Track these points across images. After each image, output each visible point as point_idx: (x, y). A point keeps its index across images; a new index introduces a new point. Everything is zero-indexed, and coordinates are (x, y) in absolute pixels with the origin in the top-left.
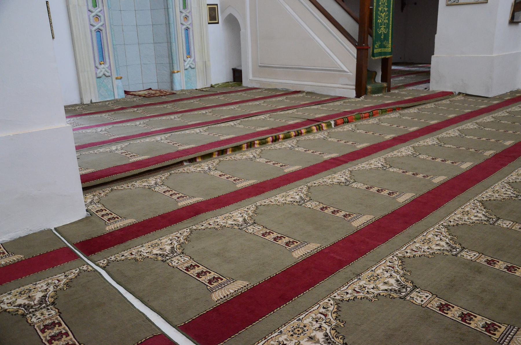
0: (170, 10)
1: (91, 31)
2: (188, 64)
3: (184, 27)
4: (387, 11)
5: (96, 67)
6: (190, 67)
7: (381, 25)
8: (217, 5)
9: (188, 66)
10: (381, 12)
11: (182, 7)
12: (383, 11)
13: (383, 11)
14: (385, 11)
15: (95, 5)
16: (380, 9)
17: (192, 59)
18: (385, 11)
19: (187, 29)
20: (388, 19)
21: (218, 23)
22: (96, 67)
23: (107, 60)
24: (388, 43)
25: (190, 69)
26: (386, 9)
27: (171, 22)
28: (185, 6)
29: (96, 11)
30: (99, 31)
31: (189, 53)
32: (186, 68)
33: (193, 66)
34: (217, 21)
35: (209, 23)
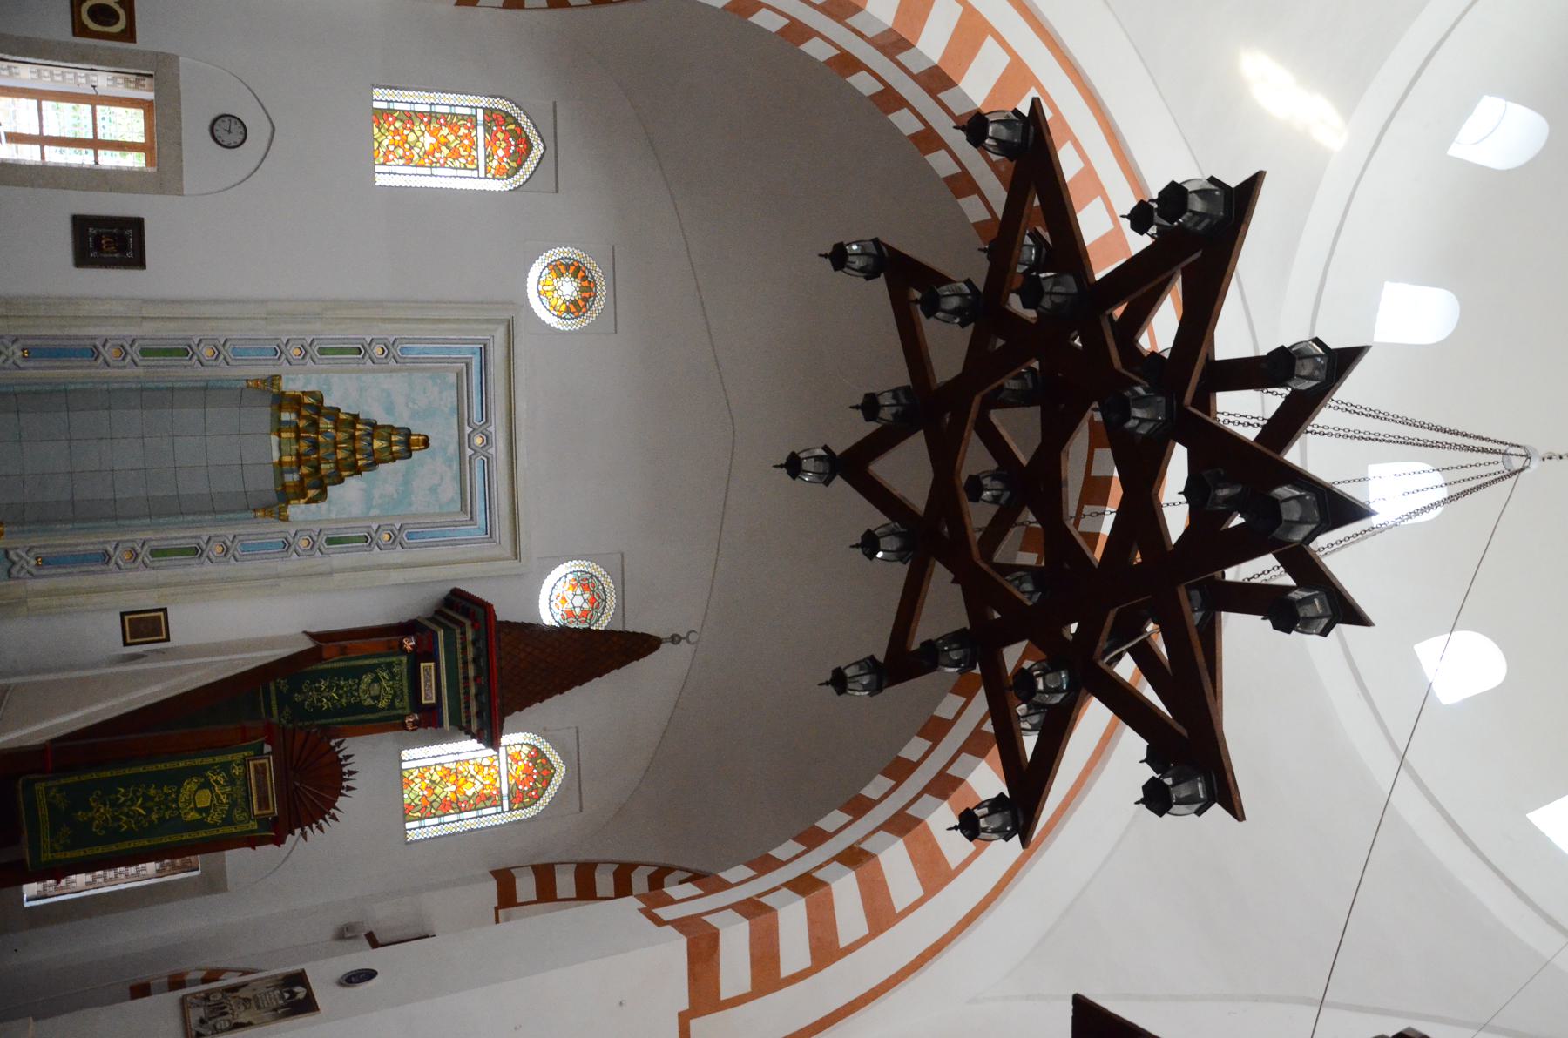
0: (148, 521)
1: (93, 338)
2: (21, 557)
3: (111, 550)
4: (151, 822)
5: (16, 340)
6: (14, 563)
7: (112, 806)
8: (168, 639)
9: (15, 559)
10: (147, 798)
11: (155, 544)
12: (150, 804)
13: (150, 804)
14: (149, 811)
15: (145, 352)
16: (152, 792)
17: (34, 571)
18: (149, 811)
19: (105, 557)
20: (130, 835)
21: (126, 644)
22: (31, 549)
23: (32, 364)
24: (67, 848)
25: (8, 564)
26: (154, 817)
27: (121, 522)
28: (155, 553)
29: (134, 352)
30: (94, 353)
31: (45, 562)
32: (12, 554)
33: (14, 571)
34: (127, 618)
35: (123, 615)
